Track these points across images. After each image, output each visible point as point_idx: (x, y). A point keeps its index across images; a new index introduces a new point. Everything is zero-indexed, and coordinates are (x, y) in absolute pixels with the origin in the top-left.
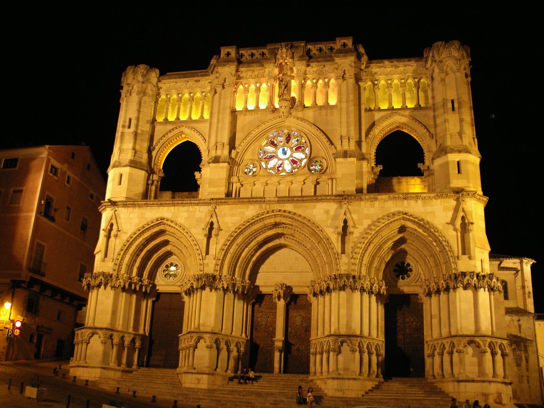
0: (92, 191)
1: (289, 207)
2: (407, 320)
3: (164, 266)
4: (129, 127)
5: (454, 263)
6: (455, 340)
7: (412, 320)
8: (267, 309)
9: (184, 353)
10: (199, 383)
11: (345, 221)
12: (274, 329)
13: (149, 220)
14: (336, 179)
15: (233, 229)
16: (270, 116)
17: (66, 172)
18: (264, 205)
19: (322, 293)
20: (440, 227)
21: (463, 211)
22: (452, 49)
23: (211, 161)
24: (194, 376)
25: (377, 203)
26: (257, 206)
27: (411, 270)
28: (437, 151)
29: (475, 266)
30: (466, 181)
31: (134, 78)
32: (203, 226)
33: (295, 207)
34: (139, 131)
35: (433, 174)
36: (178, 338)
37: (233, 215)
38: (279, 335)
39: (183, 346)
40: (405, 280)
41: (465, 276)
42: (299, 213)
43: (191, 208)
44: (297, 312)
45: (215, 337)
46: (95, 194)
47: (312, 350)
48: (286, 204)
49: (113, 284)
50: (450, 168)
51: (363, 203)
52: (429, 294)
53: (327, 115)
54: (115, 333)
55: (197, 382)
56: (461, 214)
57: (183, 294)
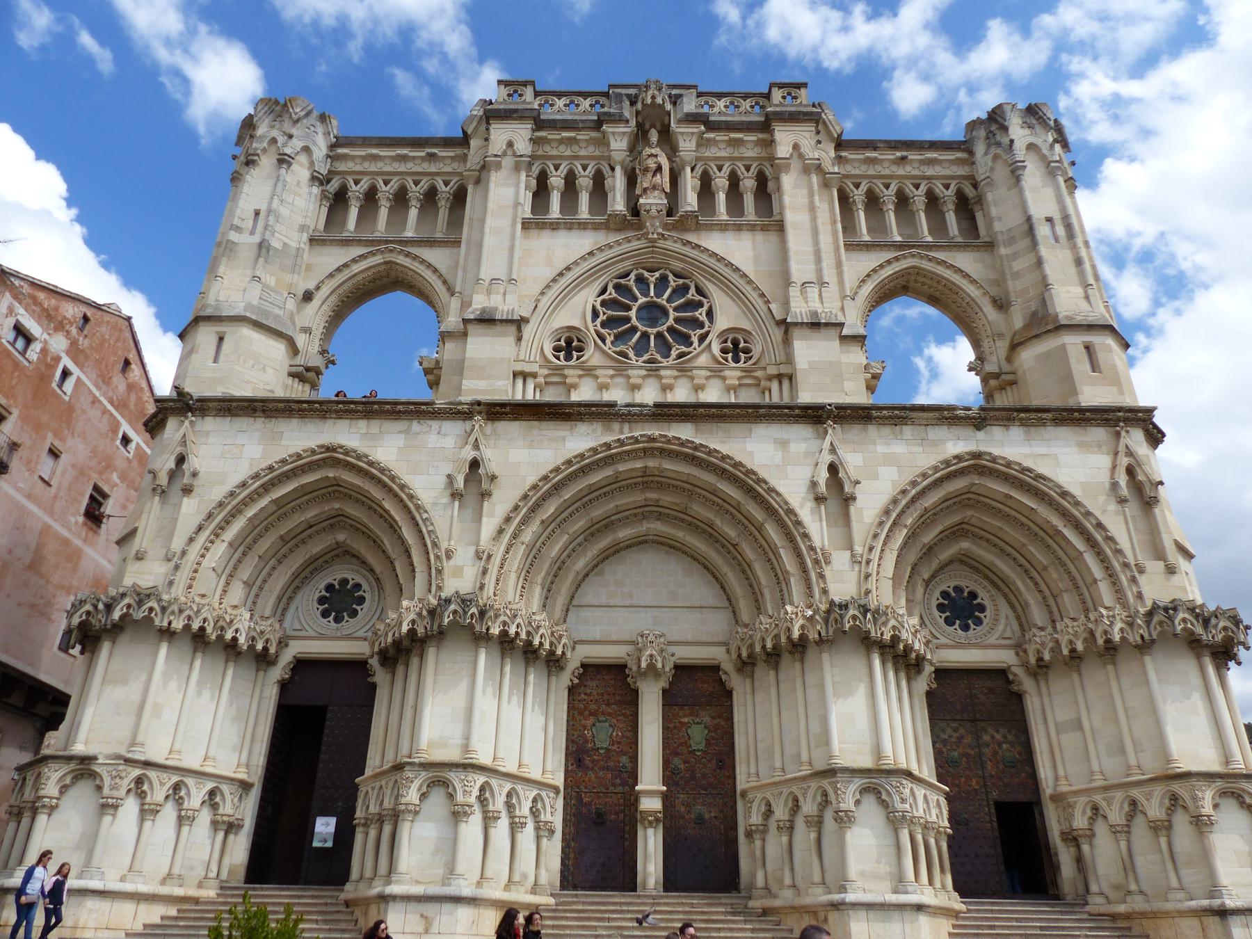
0: (126, 428)
1: (684, 432)
2: (986, 738)
3: (322, 585)
4: (252, 233)
5: (1133, 580)
6: (1176, 787)
7: (998, 737)
8: (608, 705)
9: (373, 833)
10: (427, 932)
11: (833, 469)
12: (634, 759)
13: (292, 451)
14: (791, 377)
15: (532, 479)
16: (613, 237)
17: (58, 359)
18: (616, 426)
19: (773, 657)
20: (1076, 491)
21: (1130, 453)
22: (1034, 121)
23: (472, 317)
24: (413, 906)
25: (908, 431)
26: (598, 427)
27: (982, 608)
28: (1027, 326)
29: (1184, 589)
30: (1115, 389)
31: (273, 127)
32: (448, 469)
33: (697, 430)
34: (276, 244)
35: (1013, 383)
36: (356, 788)
37: (531, 445)
38: (650, 776)
39: (372, 809)
40: (971, 632)
41: (1175, 609)
42: (712, 446)
43: (415, 426)
44: (691, 715)
45: (481, 779)
46: (132, 434)
47: (749, 816)
48: (674, 425)
49: (165, 624)
50: (1073, 360)
51: (872, 430)
52: (1040, 670)
53: (754, 243)
54: (152, 774)
55: (421, 929)
56: (1124, 461)
57: (374, 662)
